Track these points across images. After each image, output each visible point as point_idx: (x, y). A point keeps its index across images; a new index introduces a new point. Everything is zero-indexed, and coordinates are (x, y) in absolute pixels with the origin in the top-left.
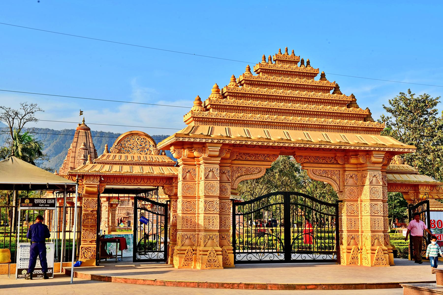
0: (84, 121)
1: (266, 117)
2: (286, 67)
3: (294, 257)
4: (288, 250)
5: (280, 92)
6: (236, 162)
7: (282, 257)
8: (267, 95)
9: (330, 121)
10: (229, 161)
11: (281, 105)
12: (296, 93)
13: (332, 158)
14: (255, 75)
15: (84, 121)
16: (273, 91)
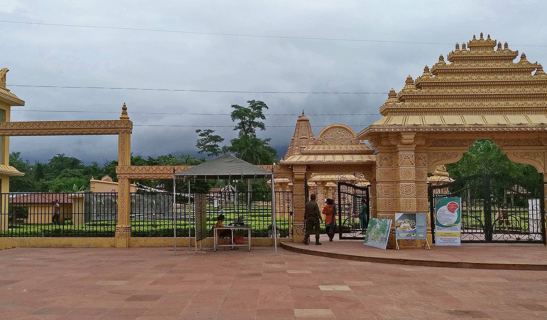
0: (303, 113)
1: (502, 104)
2: (481, 52)
3: (495, 237)
4: (488, 230)
5: (474, 78)
6: (432, 148)
7: (483, 237)
8: (462, 82)
9: (530, 103)
10: (424, 148)
11: (510, 90)
12: (492, 78)
13: (536, 140)
14: (448, 63)
15: (303, 113)
16: (466, 78)
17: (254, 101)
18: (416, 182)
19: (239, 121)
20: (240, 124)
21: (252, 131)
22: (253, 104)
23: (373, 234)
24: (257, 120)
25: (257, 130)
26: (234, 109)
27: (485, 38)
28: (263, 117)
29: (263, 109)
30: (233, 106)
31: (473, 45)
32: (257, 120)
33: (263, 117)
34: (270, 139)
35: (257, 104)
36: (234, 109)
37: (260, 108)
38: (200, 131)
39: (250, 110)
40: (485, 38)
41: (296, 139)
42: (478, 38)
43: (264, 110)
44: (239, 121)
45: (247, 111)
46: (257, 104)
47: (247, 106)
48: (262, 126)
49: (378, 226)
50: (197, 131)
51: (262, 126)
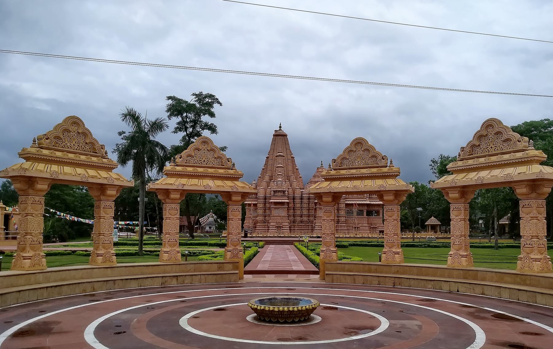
0: (280, 127)
15: (280, 127)
17: (200, 94)
19: (179, 119)
20: (178, 123)
21: (198, 135)
22: (200, 97)
24: (205, 118)
25: (206, 133)
26: (170, 102)
28: (212, 115)
29: (216, 105)
32: (205, 118)
33: (212, 115)
34: (225, 147)
35: (205, 97)
37: (210, 105)
38: (124, 133)
39: (194, 105)
41: (271, 158)
43: (216, 108)
44: (179, 119)
45: (190, 108)
46: (205, 97)
47: (191, 100)
48: (212, 129)
50: (120, 134)
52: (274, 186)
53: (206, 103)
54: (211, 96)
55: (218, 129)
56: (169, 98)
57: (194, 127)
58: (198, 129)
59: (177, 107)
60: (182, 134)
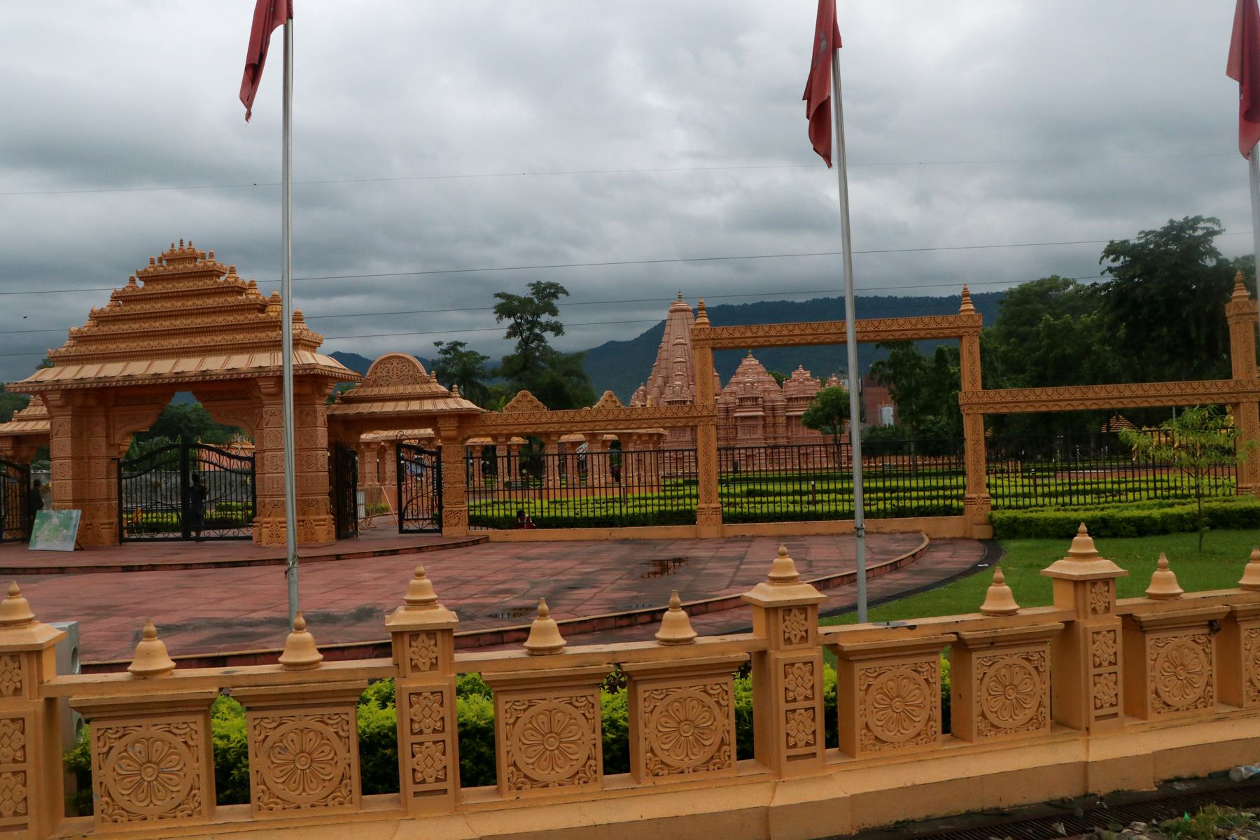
17: (539, 283)
18: (72, 458)
19: (512, 321)
20: (511, 327)
21: (540, 338)
22: (539, 288)
23: (46, 532)
25: (548, 335)
26: (499, 301)
27: (186, 245)
30: (497, 295)
31: (171, 258)
32: (545, 318)
33: (554, 312)
35: (545, 289)
36: (499, 301)
39: (530, 300)
40: (186, 245)
42: (177, 247)
44: (512, 321)
47: (525, 292)
48: (557, 329)
49: (55, 521)
50: (437, 344)
51: (557, 329)
52: (669, 395)
53: (547, 294)
54: (551, 285)
55: (565, 329)
56: (497, 295)
57: (530, 329)
58: (537, 331)
59: (508, 306)
60: (516, 341)
